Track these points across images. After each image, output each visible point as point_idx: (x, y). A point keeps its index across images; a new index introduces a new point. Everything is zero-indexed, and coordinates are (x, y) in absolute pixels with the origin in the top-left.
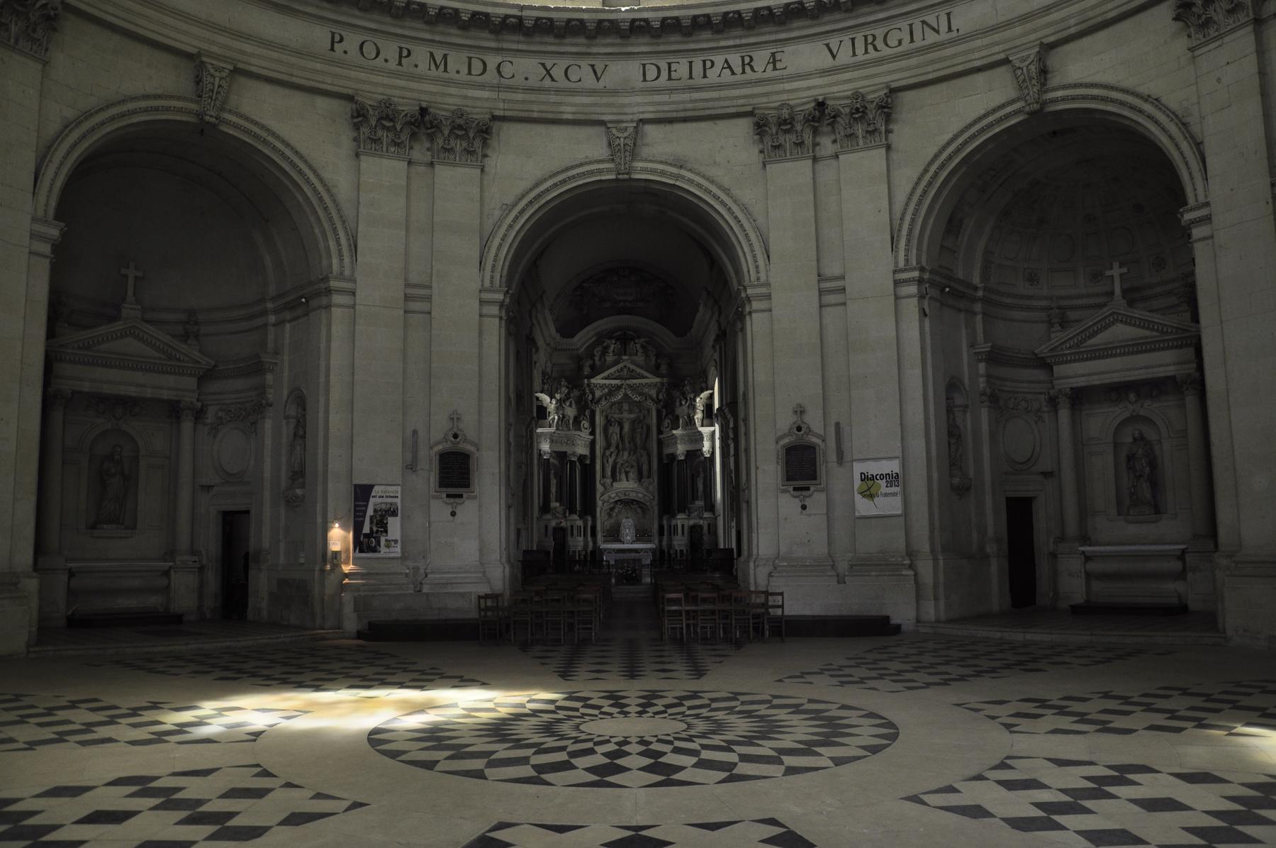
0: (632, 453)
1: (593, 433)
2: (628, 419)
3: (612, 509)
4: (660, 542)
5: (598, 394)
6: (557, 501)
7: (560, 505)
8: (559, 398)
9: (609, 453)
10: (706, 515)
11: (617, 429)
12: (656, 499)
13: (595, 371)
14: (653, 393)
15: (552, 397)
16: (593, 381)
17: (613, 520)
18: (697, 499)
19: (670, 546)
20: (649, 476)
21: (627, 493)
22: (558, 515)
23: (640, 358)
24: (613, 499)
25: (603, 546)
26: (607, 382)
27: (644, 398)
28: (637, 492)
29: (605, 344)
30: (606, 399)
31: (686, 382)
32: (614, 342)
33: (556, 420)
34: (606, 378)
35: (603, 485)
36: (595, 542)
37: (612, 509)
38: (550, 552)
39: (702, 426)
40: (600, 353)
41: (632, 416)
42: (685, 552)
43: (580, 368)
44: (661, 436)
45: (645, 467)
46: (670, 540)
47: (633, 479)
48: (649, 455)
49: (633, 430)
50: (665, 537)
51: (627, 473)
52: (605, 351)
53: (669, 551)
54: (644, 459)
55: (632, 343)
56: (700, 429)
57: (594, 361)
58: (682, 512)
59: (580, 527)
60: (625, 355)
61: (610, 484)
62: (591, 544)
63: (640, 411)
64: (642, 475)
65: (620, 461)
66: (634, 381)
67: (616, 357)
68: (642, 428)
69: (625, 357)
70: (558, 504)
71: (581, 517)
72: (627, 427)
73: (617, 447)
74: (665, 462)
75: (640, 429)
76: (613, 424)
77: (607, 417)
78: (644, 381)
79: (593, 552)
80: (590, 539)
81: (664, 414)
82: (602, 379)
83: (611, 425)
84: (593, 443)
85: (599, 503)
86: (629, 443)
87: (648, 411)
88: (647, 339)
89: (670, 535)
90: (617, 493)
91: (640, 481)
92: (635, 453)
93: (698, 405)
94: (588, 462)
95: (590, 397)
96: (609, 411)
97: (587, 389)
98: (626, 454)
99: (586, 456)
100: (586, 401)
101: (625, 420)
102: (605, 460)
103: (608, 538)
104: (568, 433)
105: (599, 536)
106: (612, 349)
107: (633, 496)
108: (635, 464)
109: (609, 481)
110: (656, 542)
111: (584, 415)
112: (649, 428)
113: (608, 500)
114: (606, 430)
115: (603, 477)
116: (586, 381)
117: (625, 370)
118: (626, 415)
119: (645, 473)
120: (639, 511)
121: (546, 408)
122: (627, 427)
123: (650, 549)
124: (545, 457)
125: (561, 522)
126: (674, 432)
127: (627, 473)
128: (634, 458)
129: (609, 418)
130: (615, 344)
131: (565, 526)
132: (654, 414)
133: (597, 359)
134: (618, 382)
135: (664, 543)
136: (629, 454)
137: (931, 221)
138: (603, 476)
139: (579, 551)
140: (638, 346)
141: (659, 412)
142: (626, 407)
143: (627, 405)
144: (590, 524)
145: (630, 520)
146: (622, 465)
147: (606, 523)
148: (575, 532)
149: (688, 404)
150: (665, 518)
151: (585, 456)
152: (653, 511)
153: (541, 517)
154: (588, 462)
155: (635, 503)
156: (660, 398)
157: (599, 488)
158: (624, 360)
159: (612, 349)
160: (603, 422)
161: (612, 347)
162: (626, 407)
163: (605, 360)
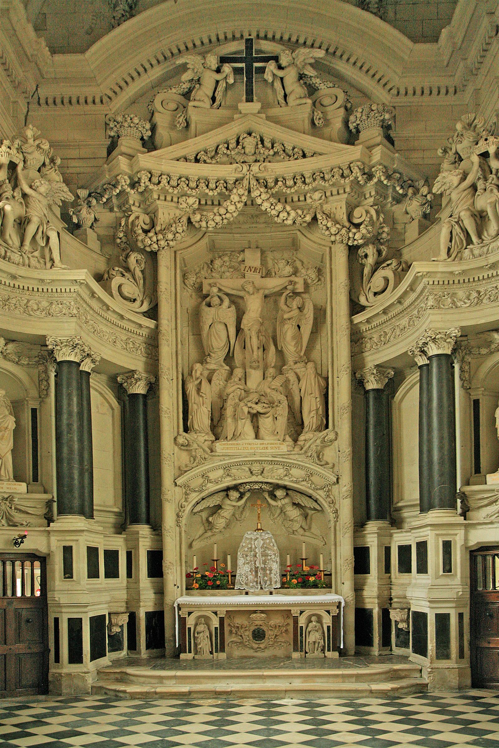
0: (271, 371)
9: (206, 373)
21: (256, 468)
28: (288, 467)
51: (255, 417)
61: (206, 446)
64: (302, 424)
73: (229, 359)
76: (216, 301)
83: (209, 305)
90: (227, 468)
91: (296, 441)
94: (140, 389)
96: (204, 273)
98: (255, 376)
99: (133, 372)
101: (250, 288)
115: (186, 430)
127: (255, 417)
128: (277, 383)
154: (140, 389)
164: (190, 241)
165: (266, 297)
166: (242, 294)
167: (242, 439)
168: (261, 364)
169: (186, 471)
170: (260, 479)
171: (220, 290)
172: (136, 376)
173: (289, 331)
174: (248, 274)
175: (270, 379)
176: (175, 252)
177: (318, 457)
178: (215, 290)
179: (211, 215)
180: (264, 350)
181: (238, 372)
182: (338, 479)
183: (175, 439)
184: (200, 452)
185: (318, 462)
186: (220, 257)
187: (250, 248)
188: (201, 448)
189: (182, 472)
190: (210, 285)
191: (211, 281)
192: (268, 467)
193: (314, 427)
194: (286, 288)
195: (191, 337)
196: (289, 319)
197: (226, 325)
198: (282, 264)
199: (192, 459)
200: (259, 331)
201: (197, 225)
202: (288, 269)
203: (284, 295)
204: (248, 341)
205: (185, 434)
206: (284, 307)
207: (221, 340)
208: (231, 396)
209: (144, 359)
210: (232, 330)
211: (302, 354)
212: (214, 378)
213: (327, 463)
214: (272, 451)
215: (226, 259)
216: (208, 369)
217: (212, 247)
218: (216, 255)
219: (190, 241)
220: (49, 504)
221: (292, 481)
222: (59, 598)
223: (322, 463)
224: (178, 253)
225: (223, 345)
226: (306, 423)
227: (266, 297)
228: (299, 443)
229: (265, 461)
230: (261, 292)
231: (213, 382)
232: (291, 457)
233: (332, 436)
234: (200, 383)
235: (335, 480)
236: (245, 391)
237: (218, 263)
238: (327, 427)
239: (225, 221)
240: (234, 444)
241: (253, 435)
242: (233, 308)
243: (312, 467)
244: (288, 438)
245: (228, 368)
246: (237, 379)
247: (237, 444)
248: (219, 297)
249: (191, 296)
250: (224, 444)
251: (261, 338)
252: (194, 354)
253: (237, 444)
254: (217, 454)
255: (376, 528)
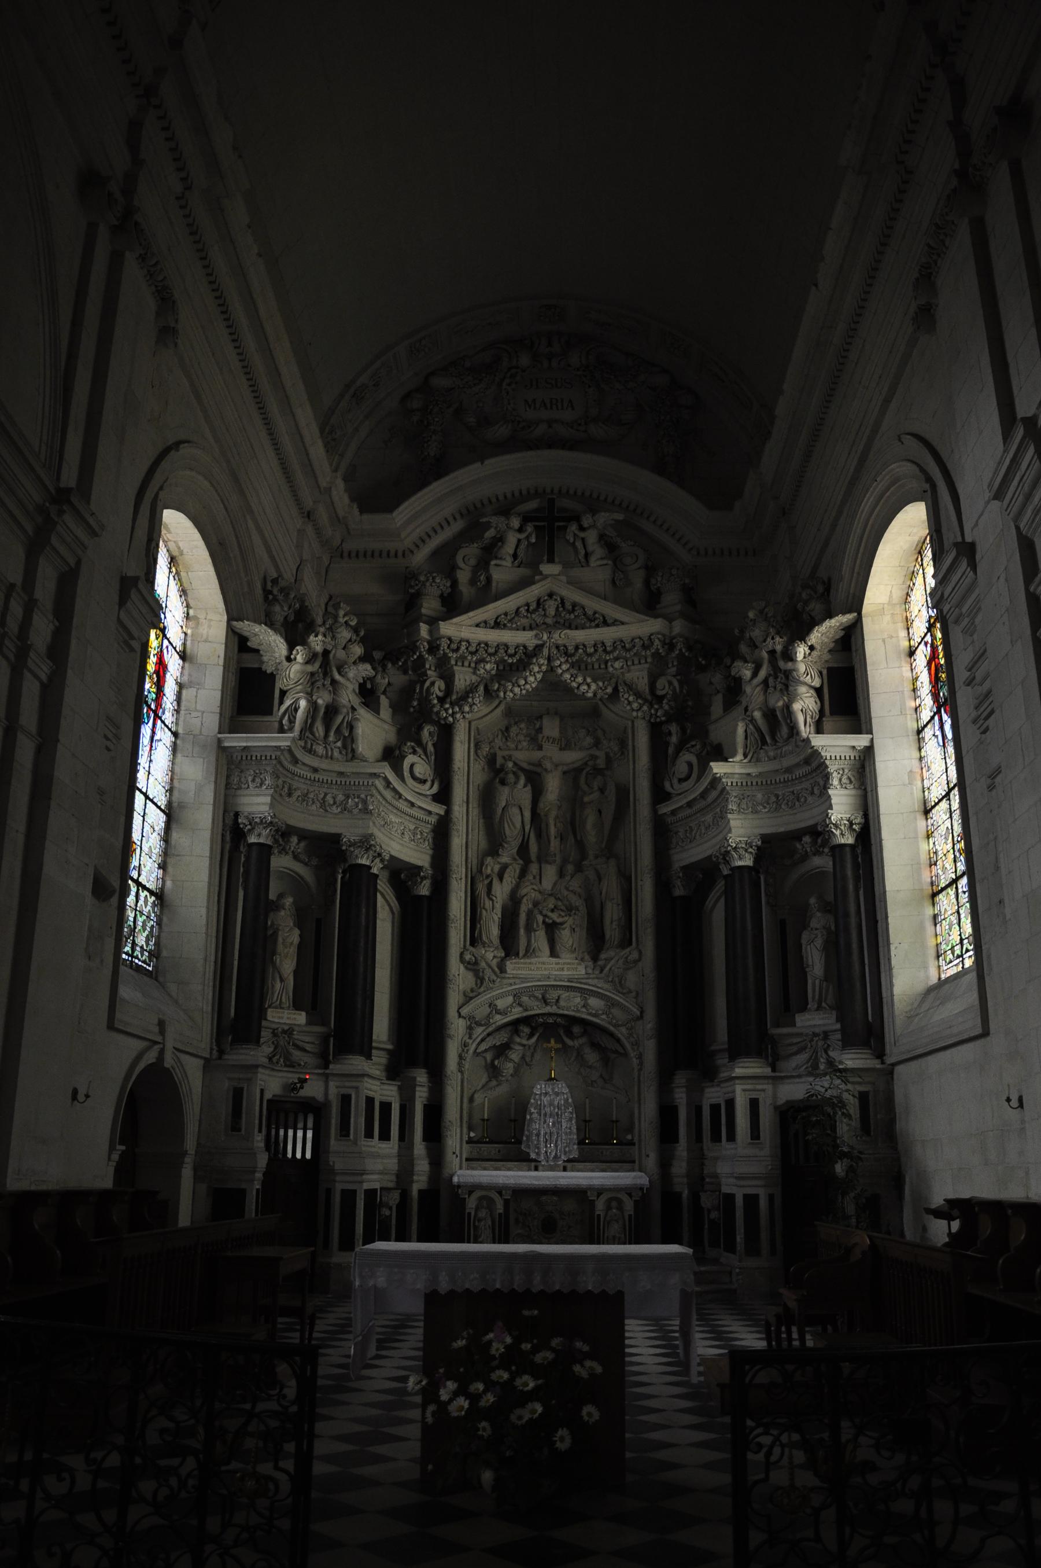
0: (570, 868)
1: (443, 796)
2: (557, 766)
3: (502, 1050)
4: (665, 1164)
5: (463, 678)
6: (297, 1006)
7: (309, 1023)
8: (319, 648)
9: (497, 868)
10: (852, 1060)
11: (523, 794)
12: (650, 1013)
13: (452, 606)
14: (639, 676)
15: (294, 639)
16: (447, 629)
17: (503, 1089)
18: (803, 1008)
19: (699, 1180)
20: (626, 942)
21: (553, 995)
22: (297, 1054)
23: (598, 572)
24: (503, 1013)
25: (464, 1175)
26: (494, 636)
27: (609, 690)
29: (490, 534)
30: (487, 691)
31: (751, 615)
32: (516, 523)
33: (300, 714)
34: (484, 624)
35: (473, 966)
36: (437, 1160)
37: (502, 1050)
38: (242, 1193)
39: (819, 730)
40: (473, 562)
41: (573, 757)
42: (763, 1203)
43: (412, 602)
44: (665, 809)
45: (612, 913)
46: (698, 1159)
47: (573, 951)
48: (627, 881)
49: (573, 801)
50: (682, 1149)
51: (551, 929)
52: (490, 551)
53: (695, 1197)
54: (611, 886)
55: (573, 527)
56: (818, 741)
57: (454, 584)
58: (748, 1054)
59: (386, 1107)
60: (551, 560)
61: (494, 963)
62: (422, 1166)
63: (597, 744)
65: (529, 892)
66: (579, 636)
67: (523, 571)
68: (602, 790)
69: (547, 569)
70: (301, 1018)
71: (393, 1072)
72: (553, 786)
73: (523, 850)
74: (679, 891)
75: (596, 795)
76: (511, 778)
77: (491, 760)
78: (608, 634)
79: (430, 1196)
80: (419, 1148)
81: (674, 739)
82: (477, 626)
83: (503, 782)
84: (441, 833)
85: (457, 1027)
86: (562, 838)
87: (623, 743)
88: (620, 517)
89: (699, 1138)
90: (516, 996)
91: (595, 959)
92: (579, 869)
93: (802, 668)
94: (424, 889)
95: (438, 688)
96: (498, 742)
97: (430, 659)
98: (550, 873)
99: (420, 868)
100: (425, 700)
101: (548, 765)
102: (481, 888)
103: (487, 1149)
104: (349, 768)
105: (454, 1140)
106: (509, 548)
107: (571, 1004)
108: (577, 902)
109: (491, 954)
110: (651, 1162)
111: (419, 742)
112: (624, 796)
113: (489, 1017)
114: (487, 799)
115: (474, 942)
116: (424, 630)
117: (551, 607)
118: (552, 752)
119: (612, 931)
120: (592, 1057)
121: (272, 677)
122: (553, 786)
123: (629, 1191)
124: (252, 839)
125: (303, 1081)
126: (718, 768)
127: (551, 929)
128: (575, 884)
129: (499, 761)
130: (520, 530)
131: (320, 1096)
132: (642, 740)
133: (463, 576)
134: (527, 638)
135: (680, 1168)
136: (561, 874)
137: (861, 892)
138: (474, 940)
139: (371, 1194)
140: (592, 537)
141: (656, 730)
142: (551, 728)
143: (557, 722)
144: (421, 1095)
145: (562, 1087)
146: (536, 904)
147: (479, 1098)
148: (358, 1121)
149: (763, 673)
150: (681, 1079)
151: (414, 870)
152: (640, 1057)
153: (221, 1052)
155: (576, 1030)
156: (660, 693)
157: (459, 977)
158: (546, 577)
159: (509, 548)
160: (479, 777)
161: (512, 539)
162: (551, 728)
163: (489, 580)
164: (485, 710)
165: (564, 773)
166: (539, 770)
167: (536, 957)
168: (558, 859)
169: (471, 998)
170: (553, 1009)
171: (515, 764)
172: (422, 874)
173: (590, 819)
174: (545, 746)
175: (568, 878)
176: (470, 723)
177: (620, 982)
178: (510, 764)
179: (509, 686)
180: (561, 839)
181: (534, 868)
182: (642, 1012)
183: (462, 954)
184: (488, 973)
185: (621, 990)
186: (516, 723)
187: (548, 714)
188: (490, 966)
189: (468, 999)
190: (504, 757)
191: (506, 753)
192: (565, 995)
193: (616, 943)
194: (586, 764)
195: (481, 821)
196: (590, 803)
197: (521, 809)
198: (582, 733)
199: (479, 982)
200: (557, 817)
201: (494, 694)
202: (589, 740)
203: (585, 772)
204: (543, 826)
205: (471, 949)
206: (585, 787)
207: (515, 828)
208: (525, 900)
209: (430, 852)
210: (527, 814)
211: (603, 846)
212: (506, 876)
213: (630, 992)
214: (570, 973)
215: (523, 725)
216: (499, 863)
217: (509, 712)
218: (512, 722)
219: (485, 710)
220: (325, 1039)
221: (590, 1014)
222: (334, 1162)
223: (625, 991)
224: (473, 724)
225: (516, 832)
226: (607, 937)
227: (564, 773)
228: (600, 963)
229: (561, 986)
230: (560, 768)
231: (504, 880)
232: (590, 981)
233: (635, 955)
234: (491, 882)
235: (638, 1013)
236: (540, 892)
237: (514, 730)
238: (630, 943)
239: (524, 692)
240: (525, 963)
241: (547, 951)
242: (529, 788)
243: (613, 996)
244: (587, 957)
245: (521, 862)
246: (531, 878)
247: (530, 963)
248: (514, 773)
249: (484, 769)
250: (515, 963)
251: (558, 825)
252: (484, 844)
253: (530, 963)
254: (507, 976)
255: (684, 1081)
